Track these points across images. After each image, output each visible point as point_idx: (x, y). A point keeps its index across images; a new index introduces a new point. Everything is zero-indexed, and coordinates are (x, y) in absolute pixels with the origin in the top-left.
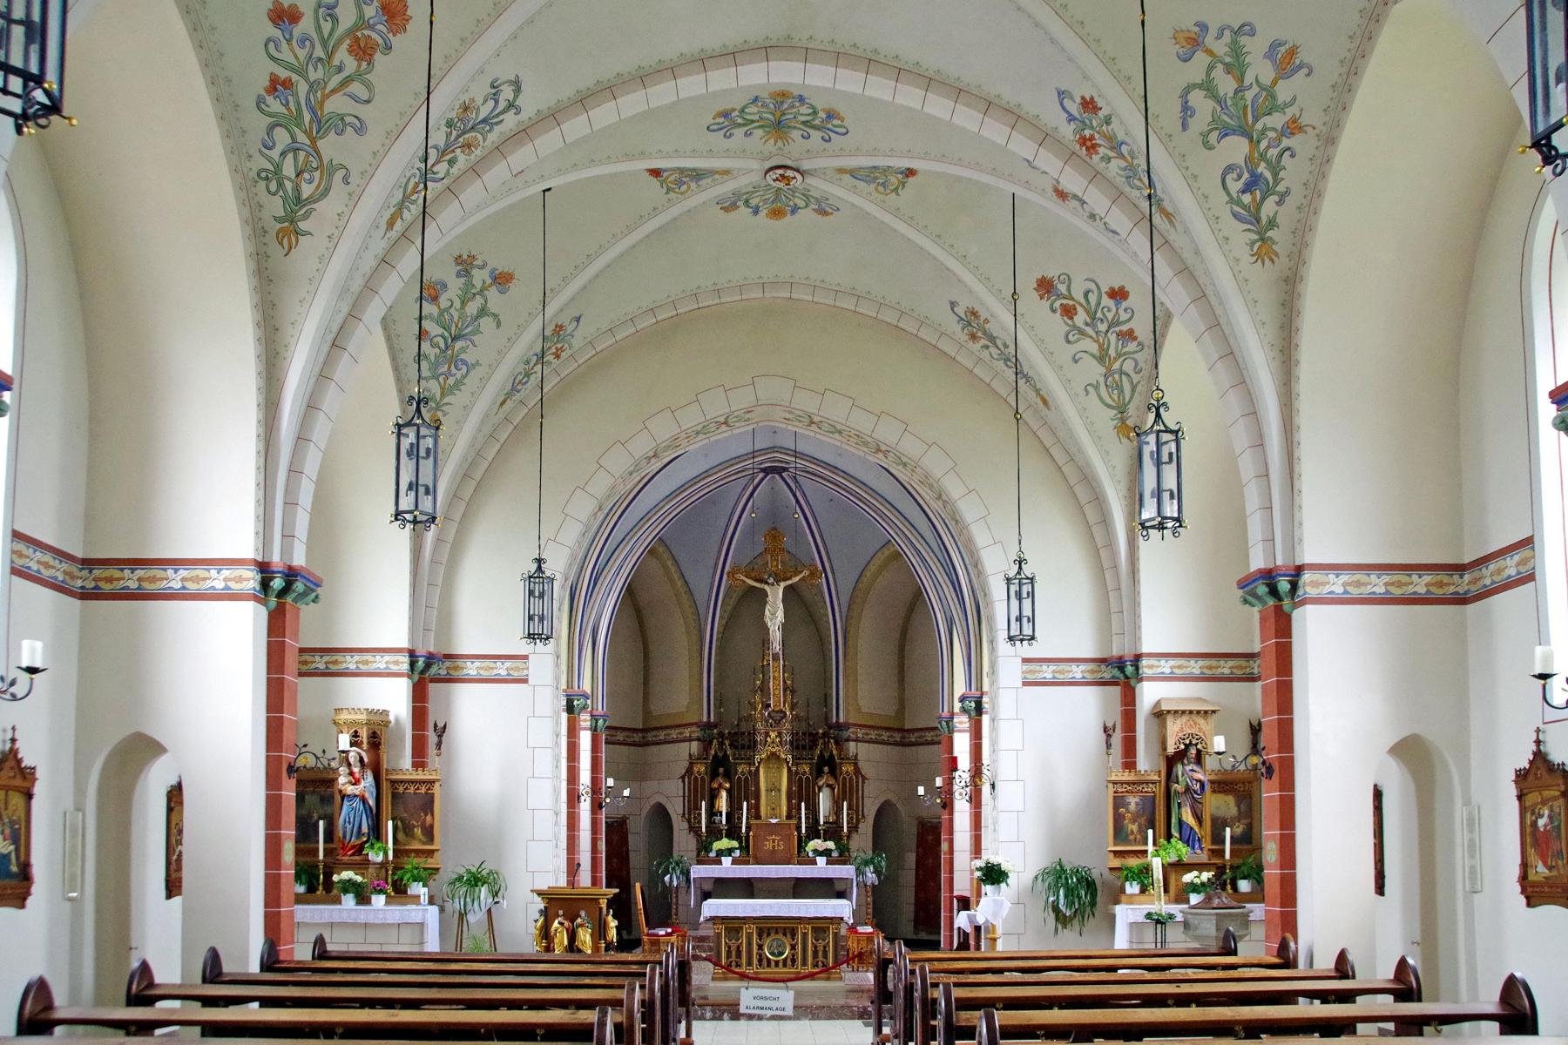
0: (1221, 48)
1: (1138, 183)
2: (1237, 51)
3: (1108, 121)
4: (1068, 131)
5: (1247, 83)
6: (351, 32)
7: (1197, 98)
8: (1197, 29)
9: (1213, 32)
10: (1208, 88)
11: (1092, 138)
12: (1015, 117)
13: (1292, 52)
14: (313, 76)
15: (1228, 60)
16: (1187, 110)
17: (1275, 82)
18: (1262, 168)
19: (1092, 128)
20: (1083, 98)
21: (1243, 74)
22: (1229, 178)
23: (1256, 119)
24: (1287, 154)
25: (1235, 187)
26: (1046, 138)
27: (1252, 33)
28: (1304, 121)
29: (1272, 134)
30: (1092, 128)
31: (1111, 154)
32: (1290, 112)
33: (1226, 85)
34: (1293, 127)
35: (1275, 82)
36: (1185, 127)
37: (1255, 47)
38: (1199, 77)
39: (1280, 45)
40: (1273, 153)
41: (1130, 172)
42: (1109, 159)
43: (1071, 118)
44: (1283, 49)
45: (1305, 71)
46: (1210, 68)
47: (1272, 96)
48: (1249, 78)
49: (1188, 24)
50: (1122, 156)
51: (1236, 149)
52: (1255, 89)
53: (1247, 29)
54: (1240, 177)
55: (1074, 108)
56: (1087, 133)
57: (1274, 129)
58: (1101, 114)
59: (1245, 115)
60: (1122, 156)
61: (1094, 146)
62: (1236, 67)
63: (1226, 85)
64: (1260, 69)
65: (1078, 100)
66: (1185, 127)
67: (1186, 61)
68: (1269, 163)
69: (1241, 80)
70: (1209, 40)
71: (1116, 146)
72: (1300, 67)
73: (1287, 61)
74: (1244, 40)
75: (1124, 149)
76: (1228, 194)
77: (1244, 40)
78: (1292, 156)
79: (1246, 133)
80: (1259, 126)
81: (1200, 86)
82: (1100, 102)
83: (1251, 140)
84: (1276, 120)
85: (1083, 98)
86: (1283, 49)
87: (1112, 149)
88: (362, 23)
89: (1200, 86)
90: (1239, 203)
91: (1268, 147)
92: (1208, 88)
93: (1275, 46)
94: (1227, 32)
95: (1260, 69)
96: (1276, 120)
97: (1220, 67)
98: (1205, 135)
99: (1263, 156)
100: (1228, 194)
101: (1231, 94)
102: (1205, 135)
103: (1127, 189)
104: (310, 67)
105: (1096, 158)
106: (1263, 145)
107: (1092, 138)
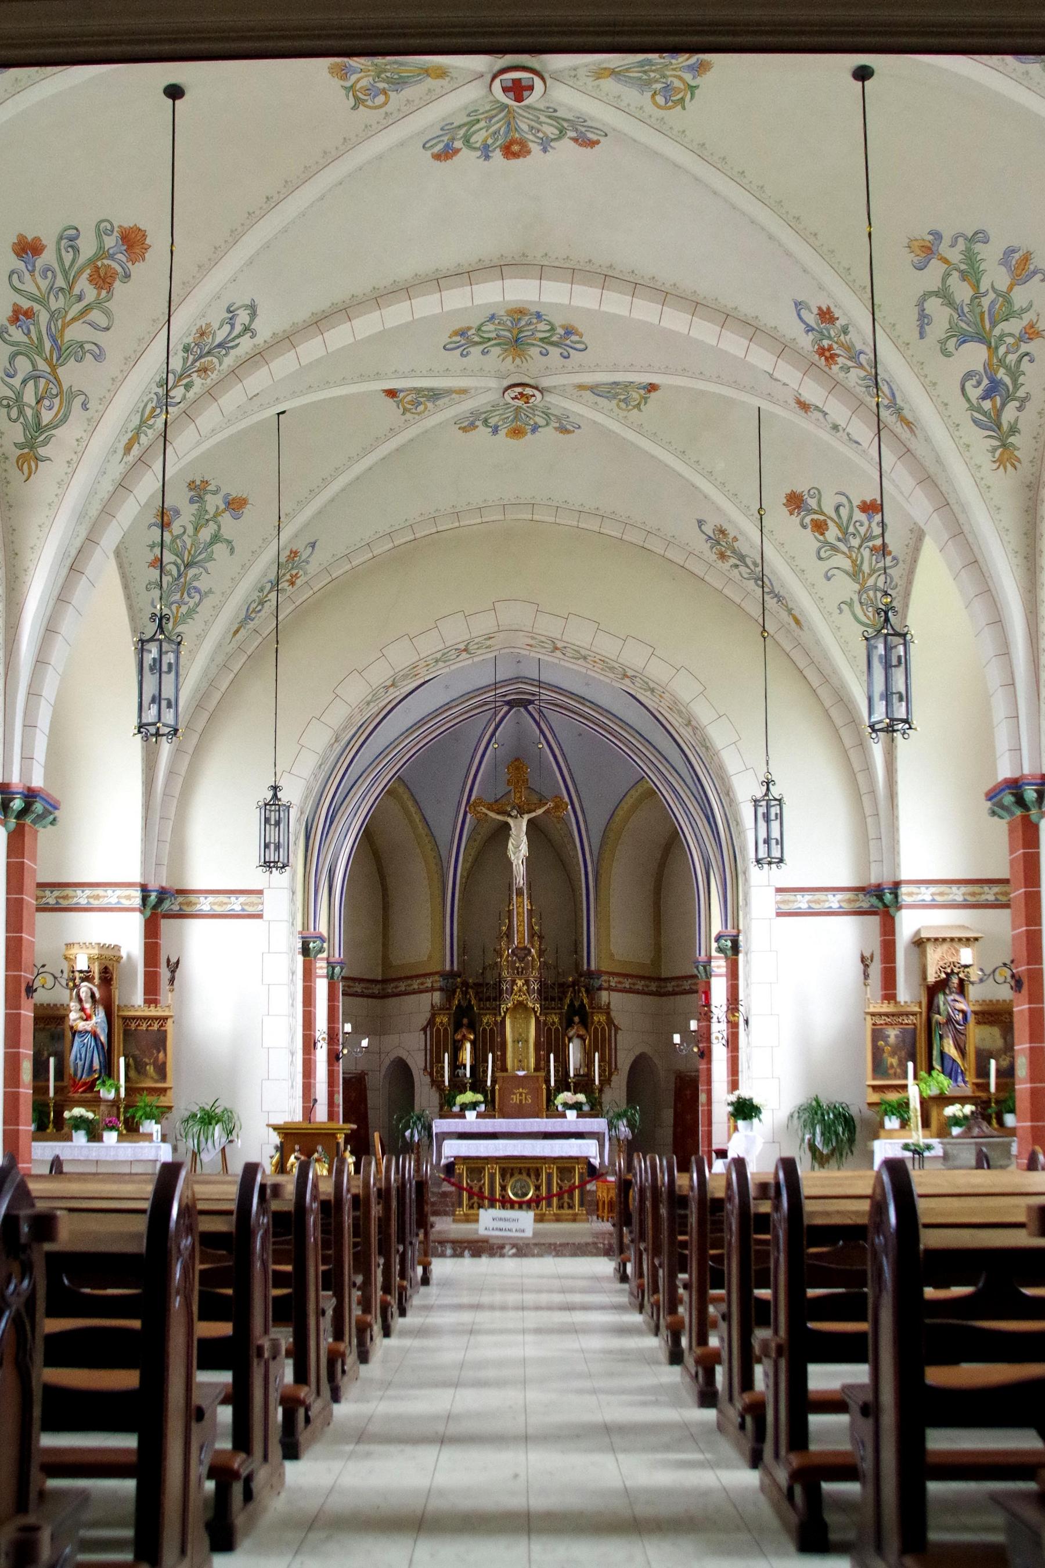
0: (955, 255)
6: (92, 261)
8: (931, 237)
14: (54, 305)
15: (963, 267)
62: (971, 274)
69: (976, 286)
70: (944, 248)
88: (102, 253)
104: (52, 297)
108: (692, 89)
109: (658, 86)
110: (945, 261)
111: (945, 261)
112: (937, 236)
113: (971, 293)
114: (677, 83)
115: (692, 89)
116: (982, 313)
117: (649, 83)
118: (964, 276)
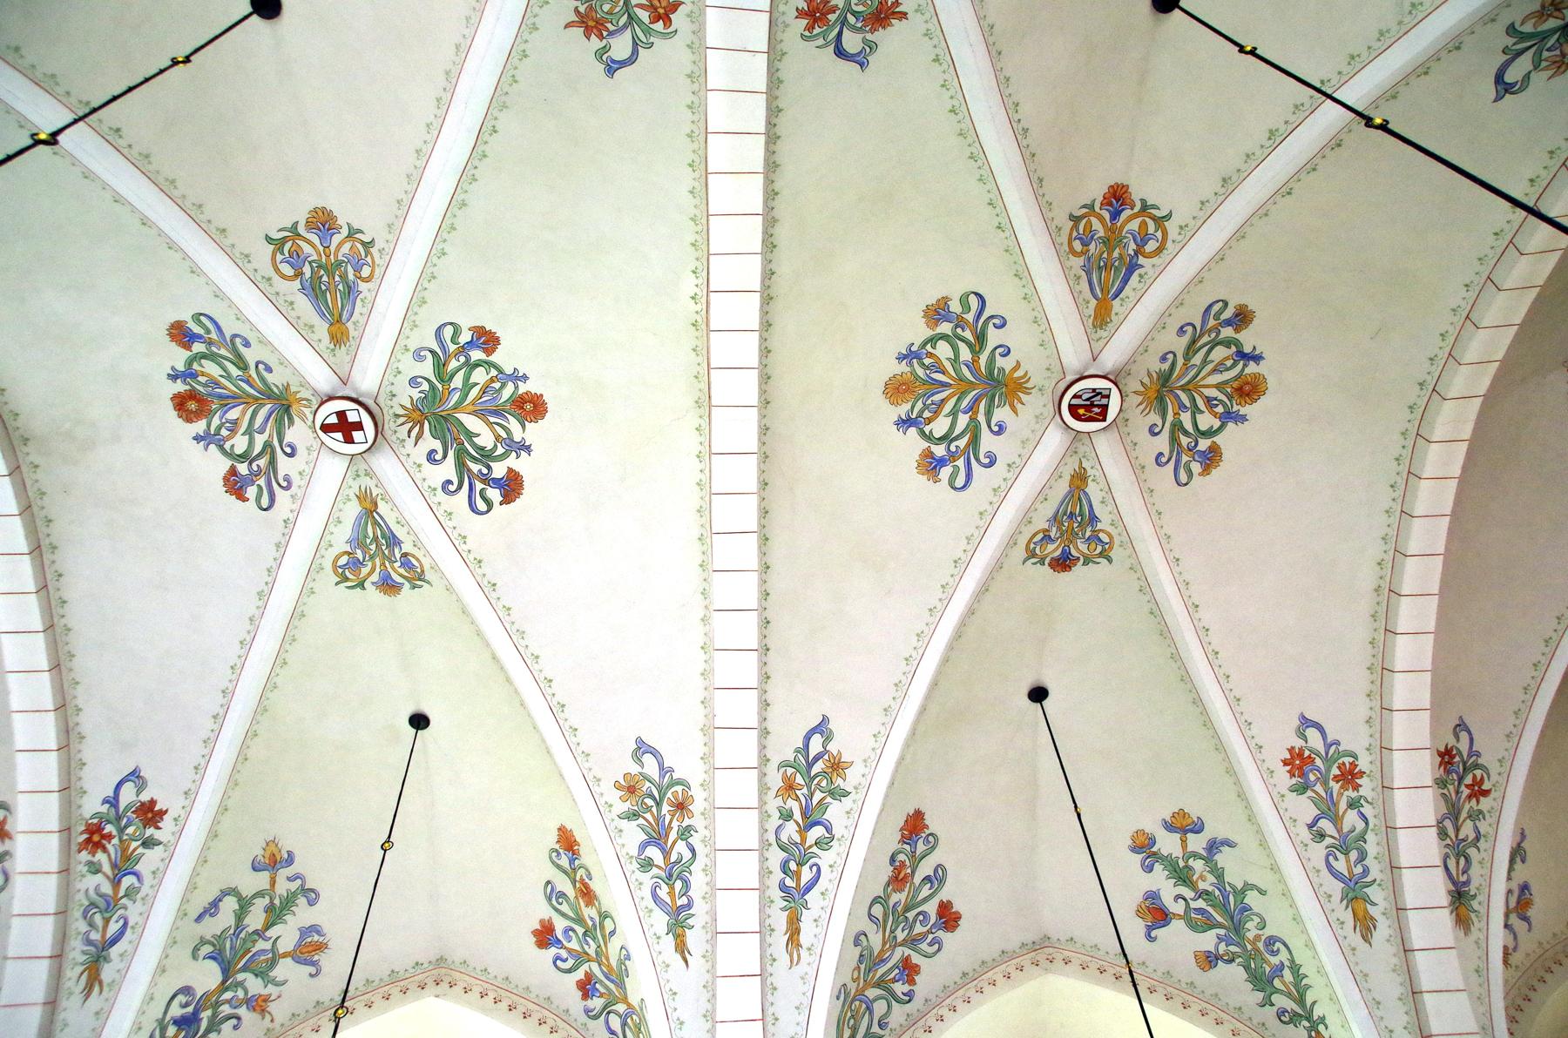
0: (283, 887)
1: (98, 919)
2: (289, 902)
3: (148, 843)
4: (92, 806)
5: (268, 934)
7: (230, 904)
9: (289, 871)
10: (244, 905)
11: (109, 837)
12: (69, 739)
13: (321, 947)
15: (277, 902)
16: (213, 908)
17: (285, 955)
18: (206, 1015)
19: (121, 830)
20: (153, 802)
21: (273, 924)
22: (176, 1002)
23: (245, 969)
24: (234, 1021)
25: (176, 1011)
26: (69, 789)
27: (311, 903)
28: (272, 1007)
29: (240, 993)
30: (121, 830)
31: (107, 868)
32: (271, 989)
33: (255, 920)
34: (259, 1005)
35: (285, 955)
36: (199, 919)
37: (302, 915)
38: (247, 892)
39: (319, 933)
40: (226, 1009)
41: (109, 905)
42: (98, 871)
43: (113, 801)
44: (316, 938)
45: (312, 970)
46: (260, 894)
47: (273, 963)
48: (272, 933)
49: (286, 845)
50: (116, 883)
51: (206, 977)
52: (267, 945)
53: (312, 896)
54: (186, 1005)
55: (128, 795)
56: (109, 828)
57: (246, 992)
58: (150, 831)
59: (243, 956)
60: (116, 883)
61: (98, 846)
62: (276, 914)
63: (255, 920)
64: (286, 935)
65: (145, 797)
66: (199, 919)
67: (254, 869)
68: (214, 1015)
69: (267, 927)
70: (283, 873)
71: (124, 867)
72: (313, 964)
73: (310, 949)
74: (302, 901)
75: (128, 881)
76: (165, 1013)
77: (302, 901)
78: (235, 1028)
79: (227, 972)
80: (240, 977)
81: (240, 898)
82: (167, 822)
83: (224, 982)
84: (254, 985)
85: (153, 802)
86: (316, 938)
87: (114, 866)
89: (240, 898)
90: (163, 1029)
91: (228, 1001)
92: (244, 905)
93: (315, 929)
94: (299, 882)
95: (286, 935)
96: (254, 985)
97: (267, 900)
98: (203, 942)
99: (217, 1004)
100: (165, 1013)
101: (250, 930)
102: (203, 942)
103: (78, 914)
105: (85, 856)
106: (228, 995)
107: (109, 837)
108: (361, 585)
109: (359, 555)
110: (273, 882)
111: (273, 882)
112: (290, 860)
113: (259, 927)
114: (365, 571)
115: (361, 585)
116: (248, 951)
117: (362, 545)
118: (270, 909)
